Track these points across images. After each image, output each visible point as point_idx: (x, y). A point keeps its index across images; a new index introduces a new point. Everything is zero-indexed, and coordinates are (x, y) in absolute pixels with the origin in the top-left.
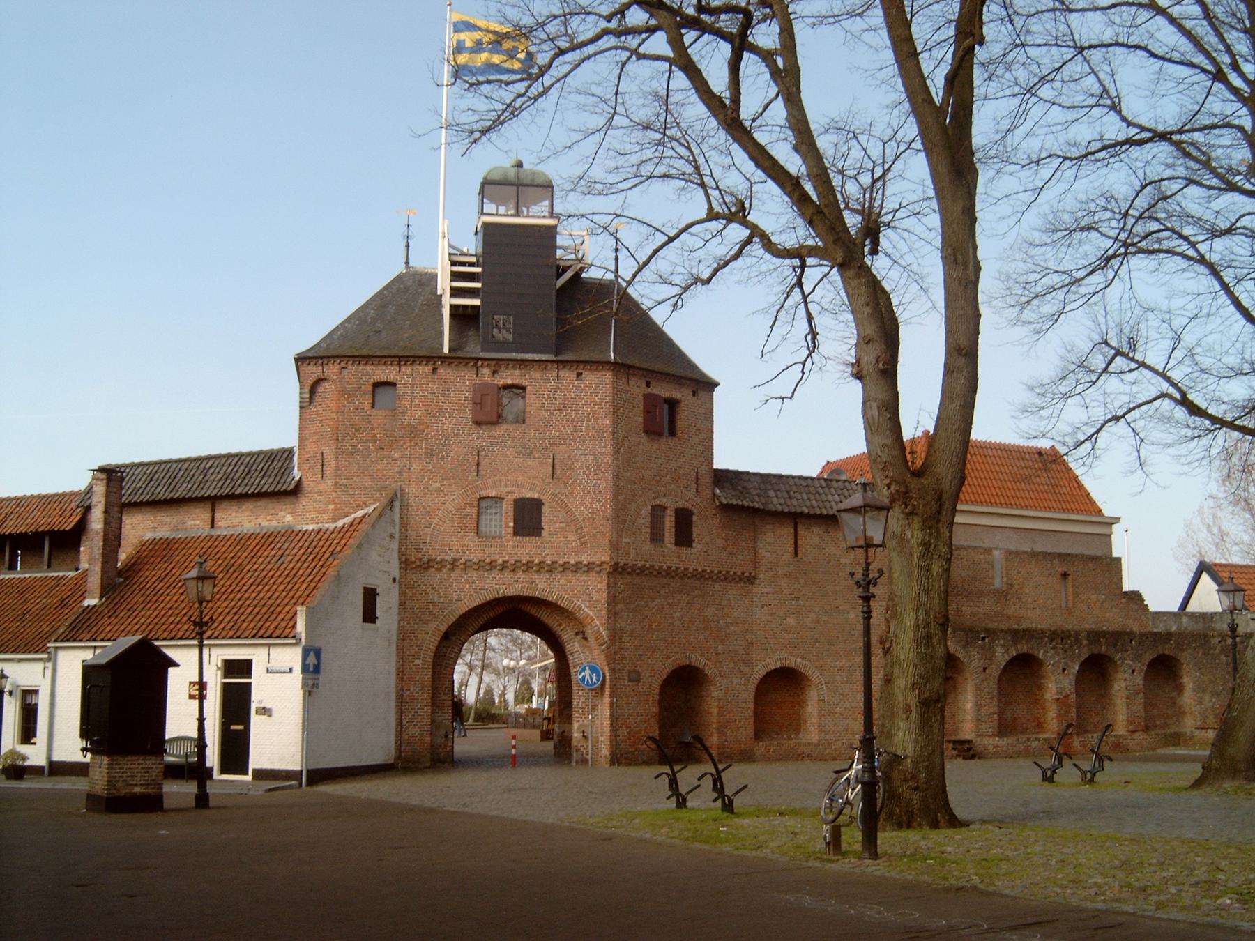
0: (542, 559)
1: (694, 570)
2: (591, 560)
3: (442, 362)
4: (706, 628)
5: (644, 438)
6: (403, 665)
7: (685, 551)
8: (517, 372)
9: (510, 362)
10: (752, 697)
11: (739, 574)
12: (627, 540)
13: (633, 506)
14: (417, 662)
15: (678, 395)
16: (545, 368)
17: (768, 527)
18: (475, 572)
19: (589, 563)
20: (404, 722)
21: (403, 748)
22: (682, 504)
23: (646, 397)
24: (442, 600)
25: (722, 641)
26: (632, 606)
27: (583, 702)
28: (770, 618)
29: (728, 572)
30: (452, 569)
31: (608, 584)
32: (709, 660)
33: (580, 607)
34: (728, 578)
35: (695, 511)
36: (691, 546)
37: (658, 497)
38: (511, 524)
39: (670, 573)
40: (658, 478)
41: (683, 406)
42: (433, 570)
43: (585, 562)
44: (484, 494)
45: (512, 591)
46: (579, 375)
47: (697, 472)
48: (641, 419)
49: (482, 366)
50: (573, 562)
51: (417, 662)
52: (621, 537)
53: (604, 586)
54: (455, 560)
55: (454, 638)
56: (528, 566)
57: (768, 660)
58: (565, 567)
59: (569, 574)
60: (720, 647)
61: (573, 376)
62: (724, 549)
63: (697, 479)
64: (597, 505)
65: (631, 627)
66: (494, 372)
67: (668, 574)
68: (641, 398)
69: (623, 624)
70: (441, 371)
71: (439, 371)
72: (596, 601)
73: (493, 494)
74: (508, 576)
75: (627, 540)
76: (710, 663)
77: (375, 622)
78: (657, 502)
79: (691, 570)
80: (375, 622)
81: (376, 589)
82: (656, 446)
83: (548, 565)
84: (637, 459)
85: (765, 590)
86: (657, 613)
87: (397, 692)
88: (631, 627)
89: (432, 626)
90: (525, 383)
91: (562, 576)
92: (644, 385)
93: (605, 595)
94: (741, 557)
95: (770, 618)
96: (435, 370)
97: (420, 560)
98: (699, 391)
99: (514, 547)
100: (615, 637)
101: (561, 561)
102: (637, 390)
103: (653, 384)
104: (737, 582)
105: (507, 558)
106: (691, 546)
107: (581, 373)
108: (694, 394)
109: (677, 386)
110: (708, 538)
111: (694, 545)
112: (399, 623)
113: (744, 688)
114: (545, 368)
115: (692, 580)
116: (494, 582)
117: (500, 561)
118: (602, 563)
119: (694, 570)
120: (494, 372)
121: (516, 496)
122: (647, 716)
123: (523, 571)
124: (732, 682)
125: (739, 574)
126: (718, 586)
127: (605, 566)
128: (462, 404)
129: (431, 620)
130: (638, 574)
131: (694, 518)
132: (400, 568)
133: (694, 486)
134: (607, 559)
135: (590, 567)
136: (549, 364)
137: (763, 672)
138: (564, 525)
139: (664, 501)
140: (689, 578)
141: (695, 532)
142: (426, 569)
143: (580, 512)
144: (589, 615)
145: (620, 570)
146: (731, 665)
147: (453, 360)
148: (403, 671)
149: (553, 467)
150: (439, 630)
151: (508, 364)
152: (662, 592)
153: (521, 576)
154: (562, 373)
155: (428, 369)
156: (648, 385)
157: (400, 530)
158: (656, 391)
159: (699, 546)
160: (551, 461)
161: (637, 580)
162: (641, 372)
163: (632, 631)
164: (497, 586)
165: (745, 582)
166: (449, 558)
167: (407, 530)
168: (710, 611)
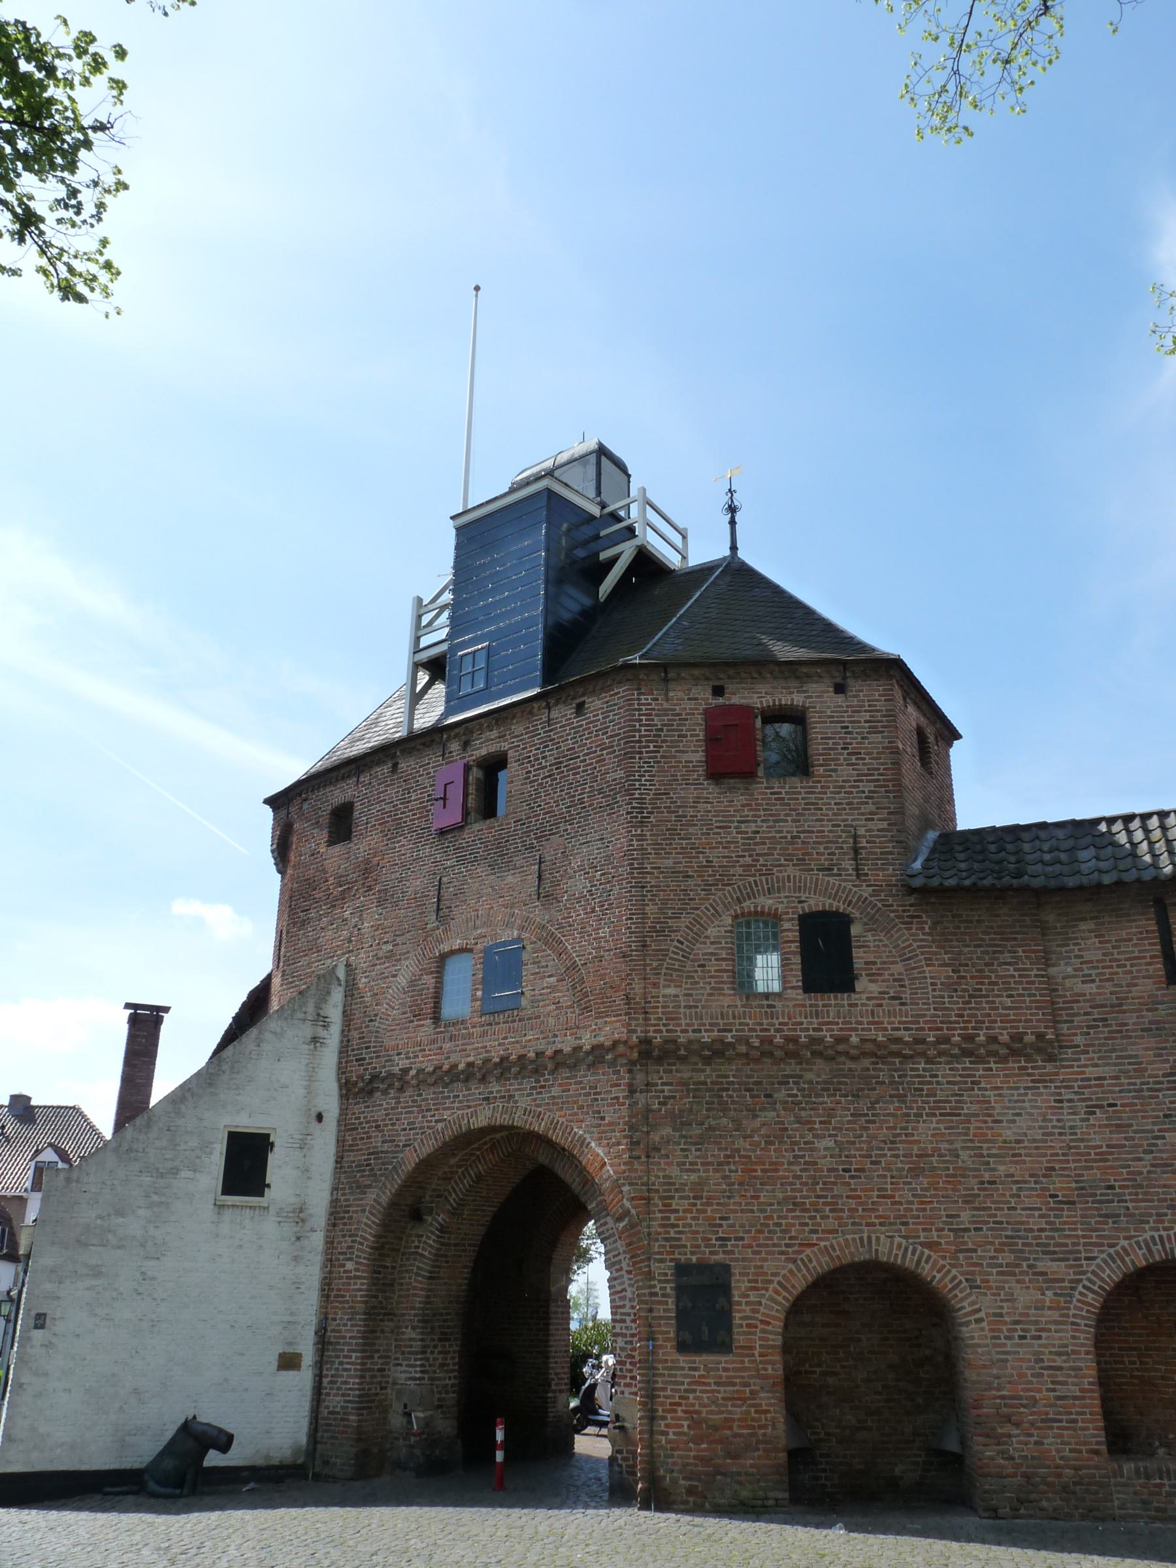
0: (522, 1052)
1: (863, 1041)
2: (595, 1041)
3: (400, 751)
4: (916, 1172)
5: (711, 790)
6: (331, 1272)
7: (834, 1002)
8: (494, 734)
9: (482, 720)
10: (1085, 1338)
11: (1005, 1038)
12: (671, 991)
13: (685, 921)
14: (350, 1265)
15: (798, 699)
16: (531, 713)
17: (1083, 926)
18: (432, 1089)
19: (594, 1048)
20: (325, 1381)
21: (319, 1434)
22: (816, 903)
23: (709, 714)
24: (386, 1147)
25: (969, 1200)
26: (696, 1131)
27: (622, 1349)
28: (1117, 1138)
29: (969, 1038)
30: (401, 1090)
31: (630, 1085)
32: (931, 1245)
33: (582, 1142)
34: (969, 1051)
35: (856, 914)
36: (852, 989)
37: (752, 895)
38: (479, 993)
39: (793, 1051)
40: (748, 860)
41: (813, 718)
42: (379, 1093)
43: (587, 1047)
44: (445, 947)
45: (482, 1119)
46: (580, 709)
47: (855, 837)
48: (699, 756)
49: (449, 739)
50: (567, 1049)
51: (350, 1265)
52: (656, 985)
53: (621, 1093)
54: (405, 1071)
55: (429, 1219)
56: (503, 1068)
57: (1125, 1243)
58: (561, 1062)
59: (565, 1073)
60: (965, 1216)
61: (570, 711)
62: (952, 987)
63: (856, 851)
64: (605, 932)
65: (694, 1177)
66: (466, 745)
67: (789, 1055)
68: (699, 719)
69: (674, 1171)
70: (403, 765)
71: (399, 766)
72: (610, 1124)
73: (457, 944)
74: (477, 1090)
75: (671, 991)
76: (934, 1256)
77: (262, 1194)
78: (748, 905)
79: (854, 1039)
80: (262, 1194)
81: (269, 1135)
82: (740, 799)
83: (532, 1062)
84: (691, 830)
85: (1090, 1072)
86: (769, 1143)
87: (320, 1322)
88: (694, 1177)
89: (371, 1195)
90: (505, 746)
91: (555, 1079)
92: (708, 694)
93: (624, 1111)
94: (1008, 1002)
95: (1117, 1138)
96: (395, 766)
97: (361, 1077)
98: (850, 682)
99: (485, 1033)
100: (649, 1199)
101: (549, 1053)
102: (689, 705)
103: (730, 687)
104: (1004, 1059)
105: (471, 1059)
106: (853, 990)
107: (584, 702)
108: (840, 689)
109: (793, 683)
110: (898, 968)
111: (859, 986)
112: (332, 1194)
113: (1055, 1315)
114: (531, 713)
115: (866, 1062)
116: (456, 1105)
117: (461, 1066)
118: (616, 1043)
119: (863, 1041)
120: (466, 745)
121: (487, 942)
122: (747, 1385)
123: (498, 1079)
124: (1011, 1299)
125: (1005, 1038)
126: (943, 1070)
127: (621, 1049)
128: (424, 807)
129: (370, 1186)
130: (707, 1060)
131: (855, 930)
132: (341, 1096)
133: (848, 864)
134: (620, 1033)
135: (597, 1055)
136: (536, 705)
137: (1111, 1275)
138: (553, 979)
139: (767, 902)
140: (854, 1058)
141: (859, 957)
142: (371, 1093)
143: (577, 947)
144: (598, 1155)
145: (656, 1053)
146: (1006, 1258)
147: (412, 744)
148: (329, 1284)
149: (540, 877)
150: (379, 1203)
151: (481, 725)
152: (781, 1095)
153: (495, 1087)
154: (554, 714)
155: (386, 769)
156: (718, 691)
157: (343, 1031)
158: (736, 700)
159: (874, 988)
160: (537, 867)
161: (708, 1074)
162: (696, 672)
163: (701, 1183)
164: (460, 1112)
165: (1029, 1058)
166: (396, 1070)
167: (349, 1031)
168: (926, 1131)
